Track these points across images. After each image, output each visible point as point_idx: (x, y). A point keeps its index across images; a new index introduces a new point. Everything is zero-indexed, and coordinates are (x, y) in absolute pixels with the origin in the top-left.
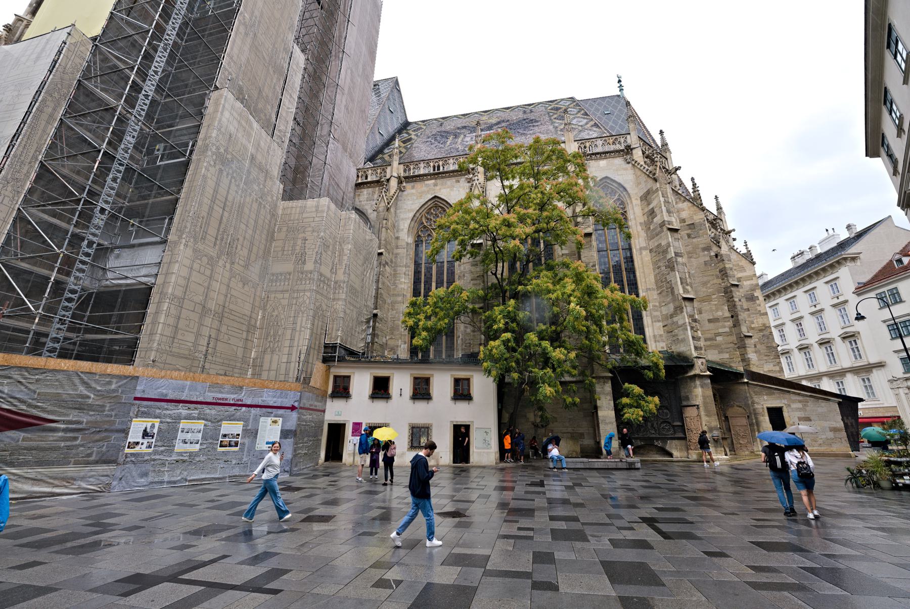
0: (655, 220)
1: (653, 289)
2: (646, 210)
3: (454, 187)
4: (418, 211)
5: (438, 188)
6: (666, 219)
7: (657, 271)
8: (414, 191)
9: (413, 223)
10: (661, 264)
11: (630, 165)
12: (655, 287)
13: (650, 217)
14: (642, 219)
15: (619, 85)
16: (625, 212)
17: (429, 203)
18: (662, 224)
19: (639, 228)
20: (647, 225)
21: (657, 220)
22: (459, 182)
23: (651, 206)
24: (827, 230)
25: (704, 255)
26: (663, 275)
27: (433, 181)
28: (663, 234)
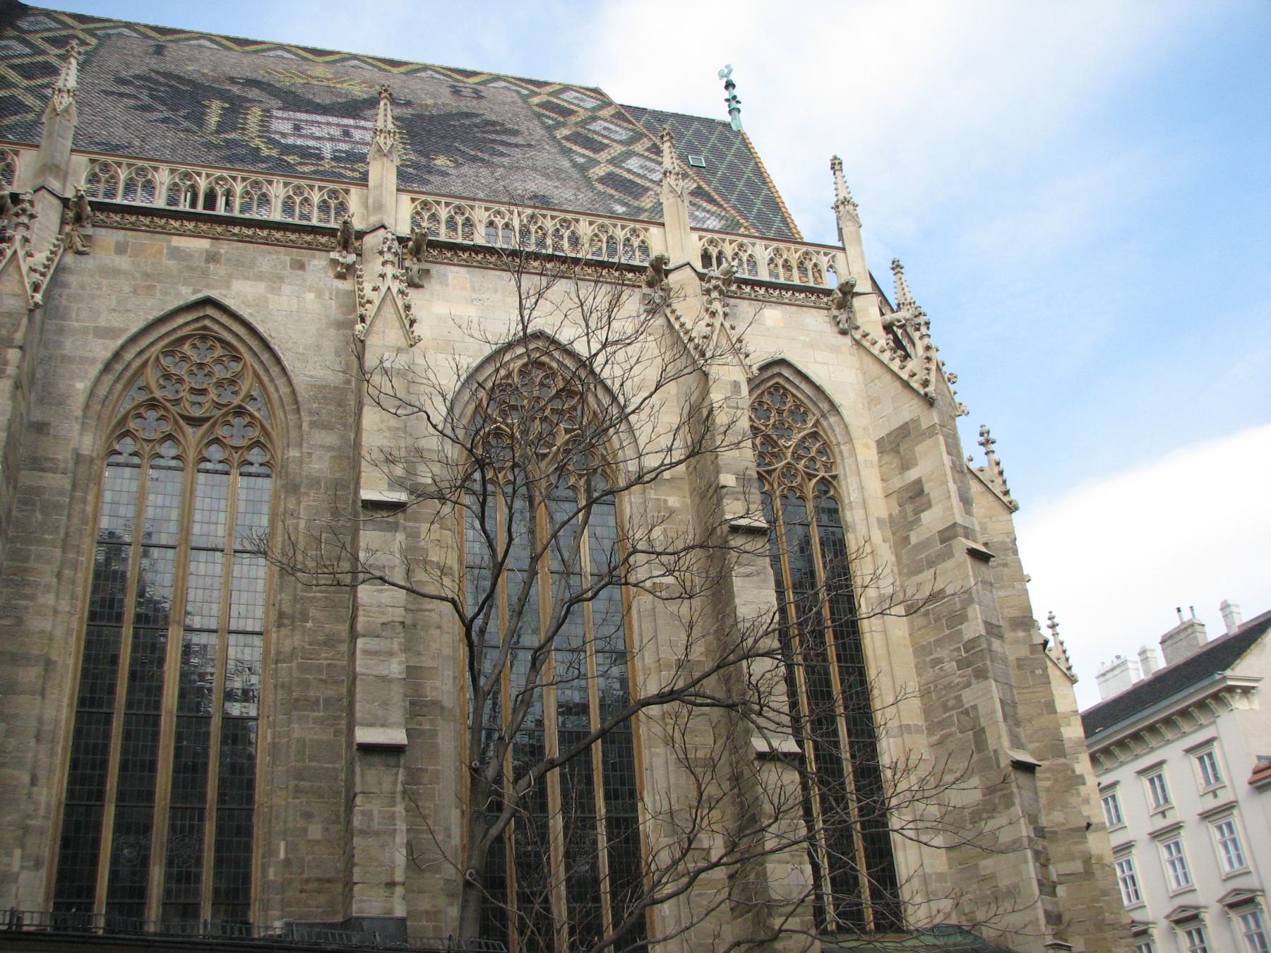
0: (926, 517)
1: (918, 730)
2: (897, 483)
3: (281, 279)
4: (134, 339)
5: (220, 270)
6: (959, 520)
7: (930, 673)
8: (123, 262)
9: (108, 379)
10: (942, 653)
11: (847, 340)
12: (921, 722)
13: (909, 508)
14: (881, 508)
15: (727, 95)
16: (835, 477)
17: (180, 321)
18: (948, 534)
19: (877, 536)
20: (901, 528)
21: (932, 520)
22: (301, 266)
23: (913, 475)
24: (1179, 610)
25: (1017, 641)
26: (949, 687)
27: (205, 244)
28: (949, 564)
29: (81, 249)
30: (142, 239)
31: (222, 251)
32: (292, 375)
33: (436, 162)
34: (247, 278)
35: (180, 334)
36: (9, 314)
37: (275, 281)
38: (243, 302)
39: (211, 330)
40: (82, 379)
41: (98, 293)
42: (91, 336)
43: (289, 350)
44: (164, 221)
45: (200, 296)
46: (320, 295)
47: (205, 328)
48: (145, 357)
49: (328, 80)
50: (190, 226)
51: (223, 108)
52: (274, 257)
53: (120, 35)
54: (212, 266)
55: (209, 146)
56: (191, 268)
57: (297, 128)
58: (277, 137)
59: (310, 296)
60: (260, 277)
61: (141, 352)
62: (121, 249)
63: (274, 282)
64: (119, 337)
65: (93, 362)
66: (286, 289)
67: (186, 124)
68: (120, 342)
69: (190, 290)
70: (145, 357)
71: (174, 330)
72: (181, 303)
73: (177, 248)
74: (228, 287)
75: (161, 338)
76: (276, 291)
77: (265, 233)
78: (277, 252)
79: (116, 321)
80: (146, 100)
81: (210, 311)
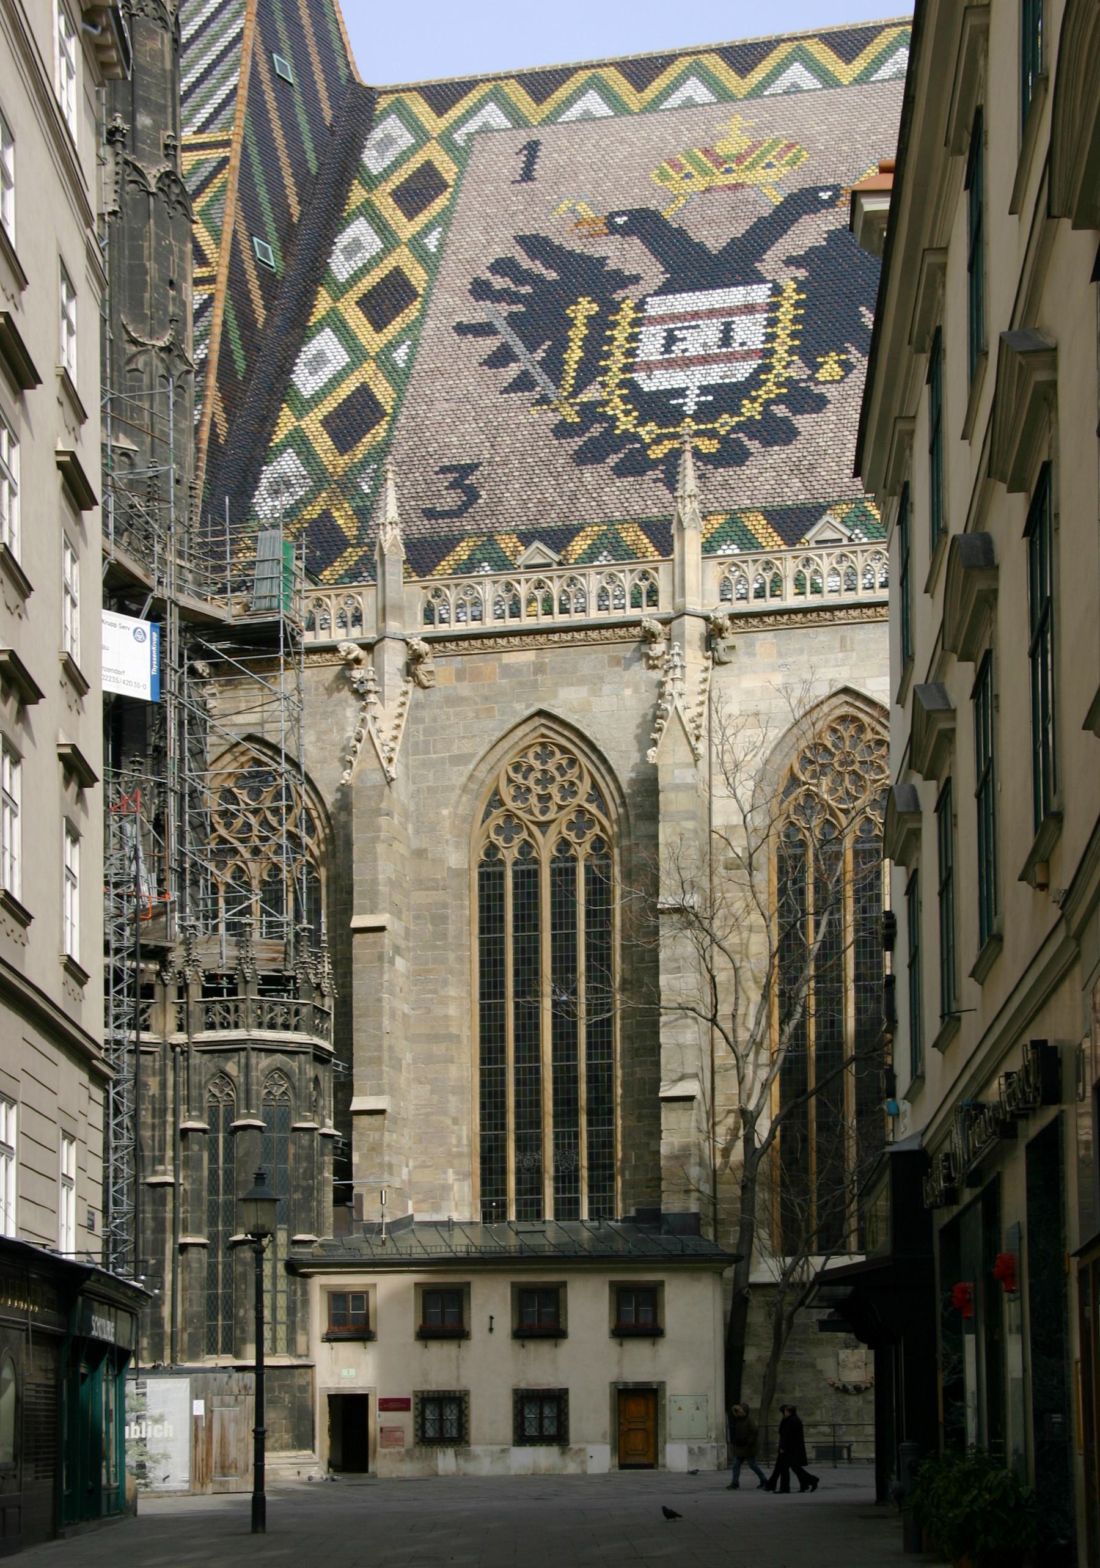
3: (601, 679)
4: (482, 760)
8: (464, 689)
17: (520, 732)
27: (530, 656)
29: (427, 684)
30: (477, 662)
31: (547, 660)
32: (617, 772)
33: (822, 375)
34: (572, 685)
35: (522, 745)
36: (375, 787)
37: (596, 682)
38: (570, 710)
39: (548, 737)
40: (446, 806)
41: (448, 723)
42: (448, 765)
43: (613, 749)
44: (492, 641)
45: (533, 710)
46: (636, 690)
47: (543, 736)
48: (495, 773)
49: (739, 159)
50: (515, 641)
51: (591, 320)
52: (593, 657)
53: (486, 130)
54: (539, 677)
55: (563, 430)
56: (521, 684)
57: (671, 339)
58: (639, 377)
59: (628, 692)
60: (582, 681)
61: (492, 768)
62: (460, 676)
63: (595, 684)
64: (470, 761)
65: (452, 788)
66: (607, 689)
67: (541, 378)
68: (471, 767)
69: (523, 706)
70: (495, 773)
71: (517, 743)
72: (518, 720)
73: (507, 665)
74: (555, 695)
75: (506, 752)
76: (595, 692)
77: (582, 634)
78: (595, 652)
79: (466, 747)
80: (507, 335)
81: (543, 721)
